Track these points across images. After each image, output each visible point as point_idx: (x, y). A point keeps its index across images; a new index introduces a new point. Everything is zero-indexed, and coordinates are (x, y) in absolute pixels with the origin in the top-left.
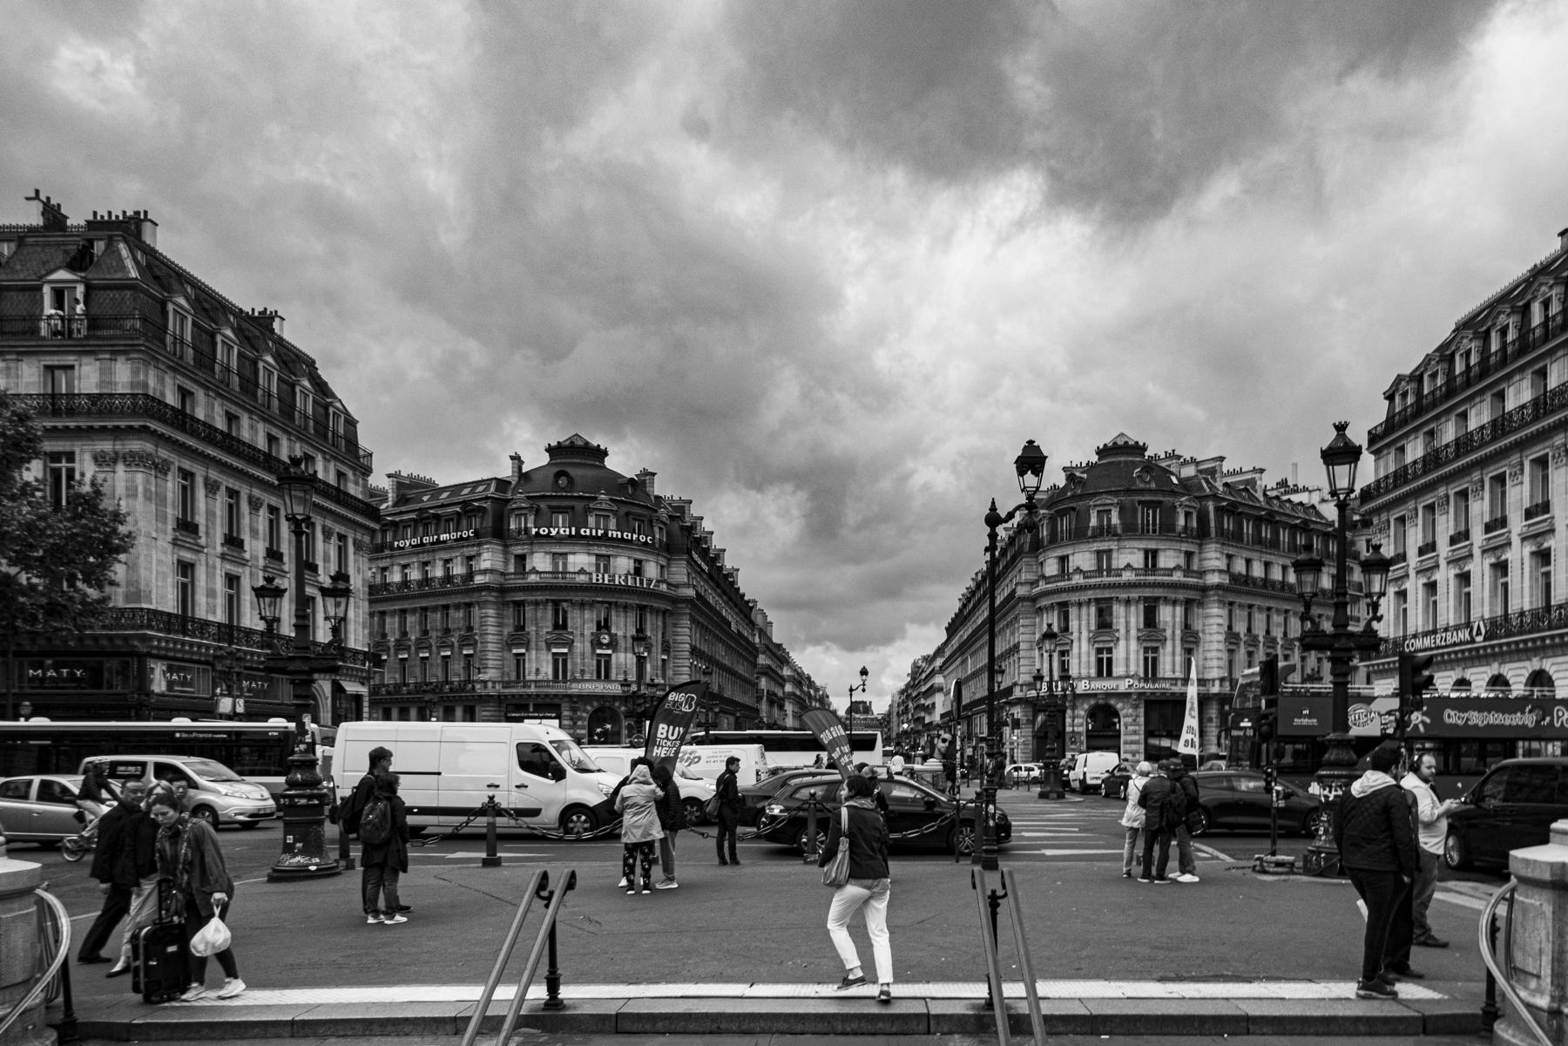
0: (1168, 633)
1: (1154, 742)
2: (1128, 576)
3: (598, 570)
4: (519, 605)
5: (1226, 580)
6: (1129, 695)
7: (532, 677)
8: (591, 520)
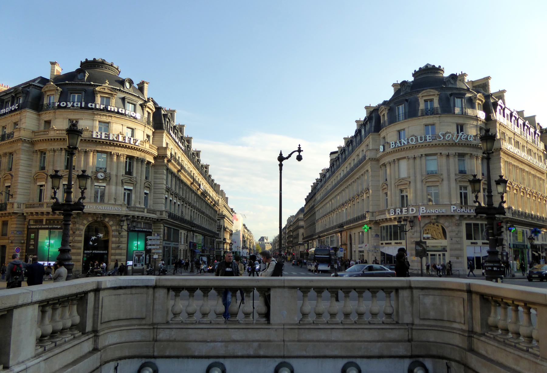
4: (43, 153)
6: (452, 216)
8: (98, 99)
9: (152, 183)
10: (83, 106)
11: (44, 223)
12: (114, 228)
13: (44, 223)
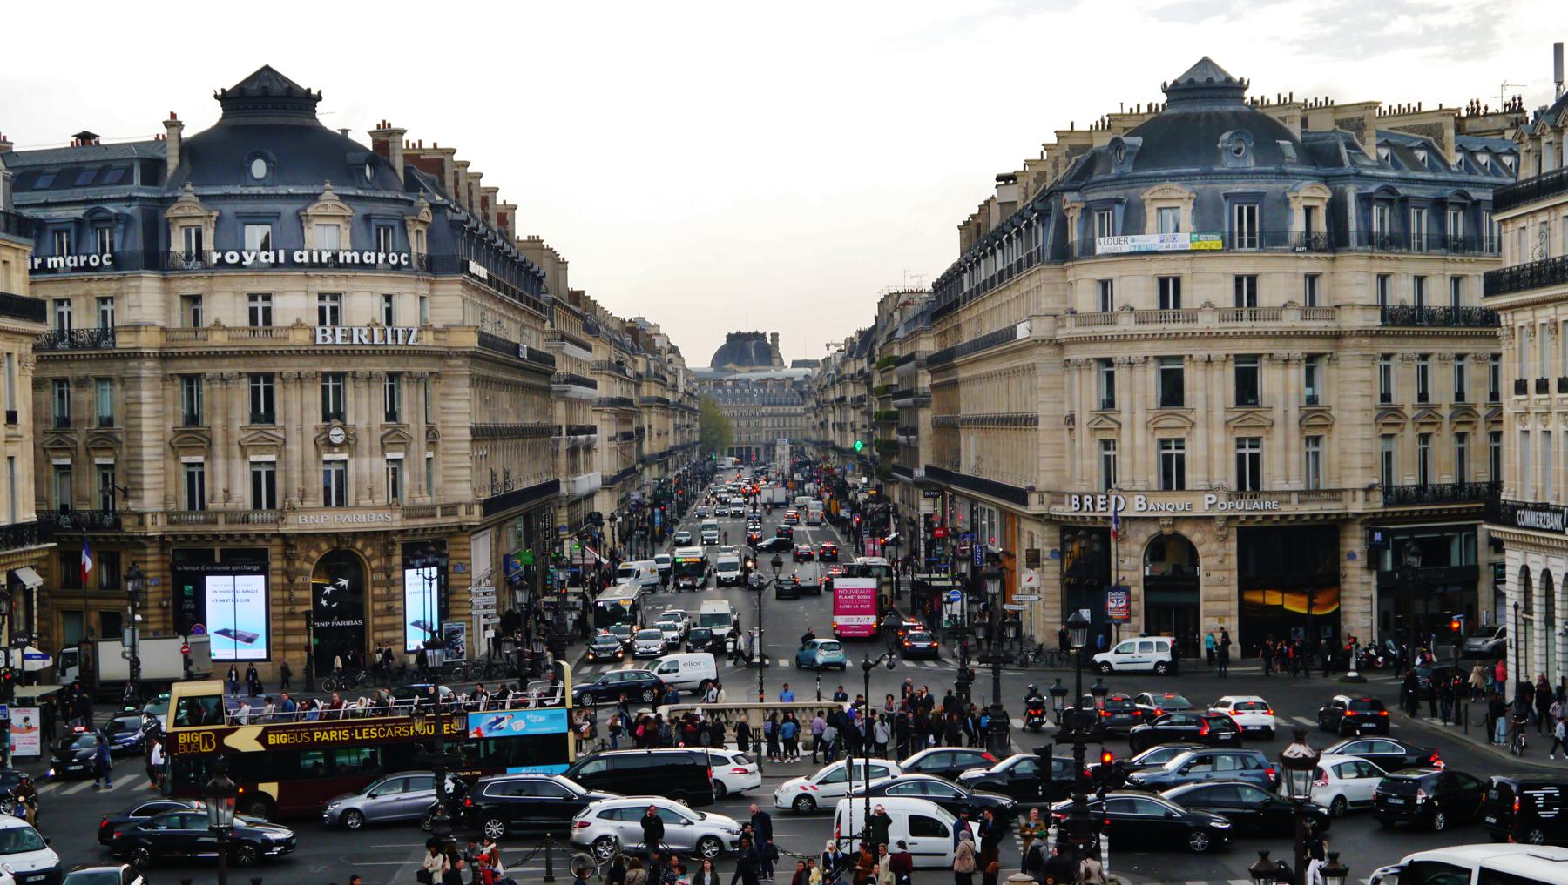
0: (1277, 415)
1: (1256, 597)
2: (1207, 322)
3: (322, 322)
5: (1374, 320)
7: (218, 505)
9: (439, 426)
10: (282, 260)
11: (218, 559)
12: (375, 563)
13: (218, 559)
